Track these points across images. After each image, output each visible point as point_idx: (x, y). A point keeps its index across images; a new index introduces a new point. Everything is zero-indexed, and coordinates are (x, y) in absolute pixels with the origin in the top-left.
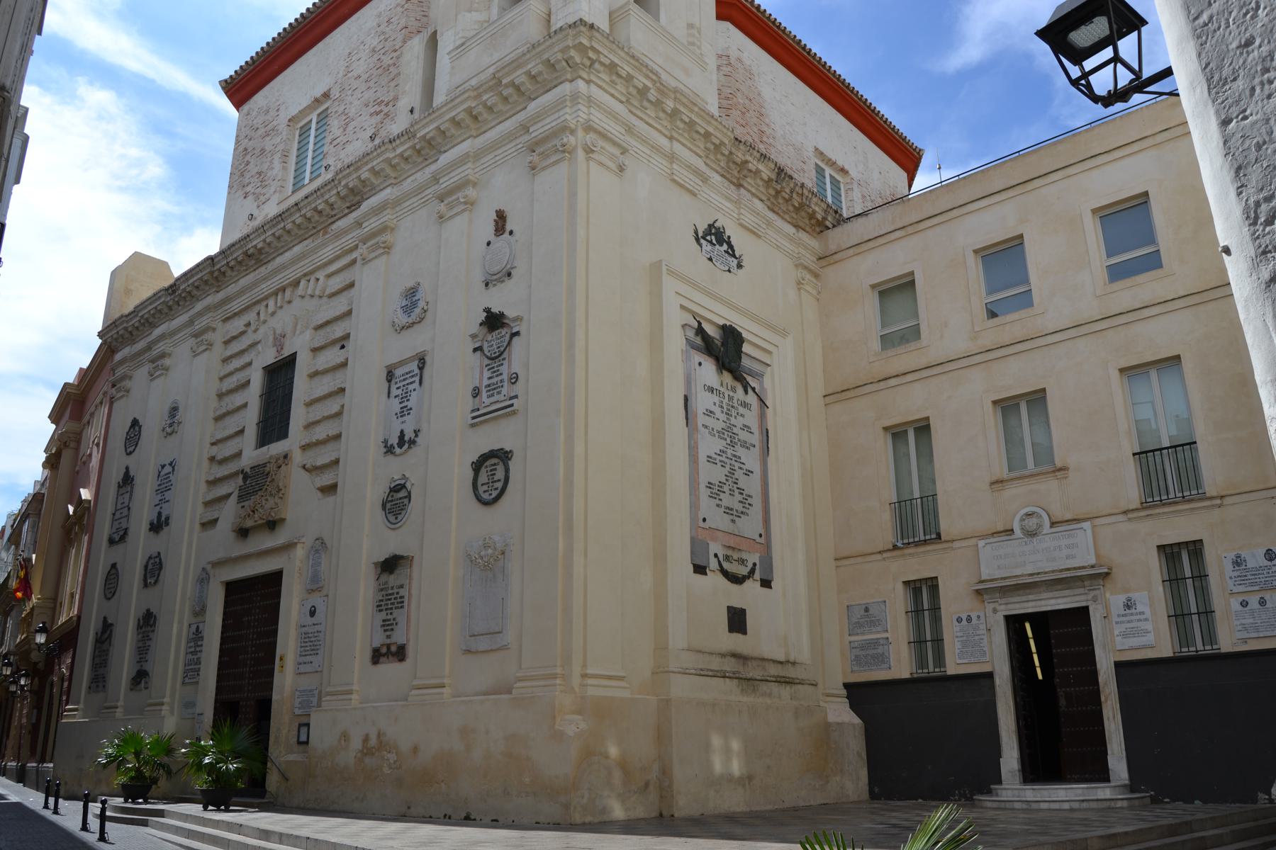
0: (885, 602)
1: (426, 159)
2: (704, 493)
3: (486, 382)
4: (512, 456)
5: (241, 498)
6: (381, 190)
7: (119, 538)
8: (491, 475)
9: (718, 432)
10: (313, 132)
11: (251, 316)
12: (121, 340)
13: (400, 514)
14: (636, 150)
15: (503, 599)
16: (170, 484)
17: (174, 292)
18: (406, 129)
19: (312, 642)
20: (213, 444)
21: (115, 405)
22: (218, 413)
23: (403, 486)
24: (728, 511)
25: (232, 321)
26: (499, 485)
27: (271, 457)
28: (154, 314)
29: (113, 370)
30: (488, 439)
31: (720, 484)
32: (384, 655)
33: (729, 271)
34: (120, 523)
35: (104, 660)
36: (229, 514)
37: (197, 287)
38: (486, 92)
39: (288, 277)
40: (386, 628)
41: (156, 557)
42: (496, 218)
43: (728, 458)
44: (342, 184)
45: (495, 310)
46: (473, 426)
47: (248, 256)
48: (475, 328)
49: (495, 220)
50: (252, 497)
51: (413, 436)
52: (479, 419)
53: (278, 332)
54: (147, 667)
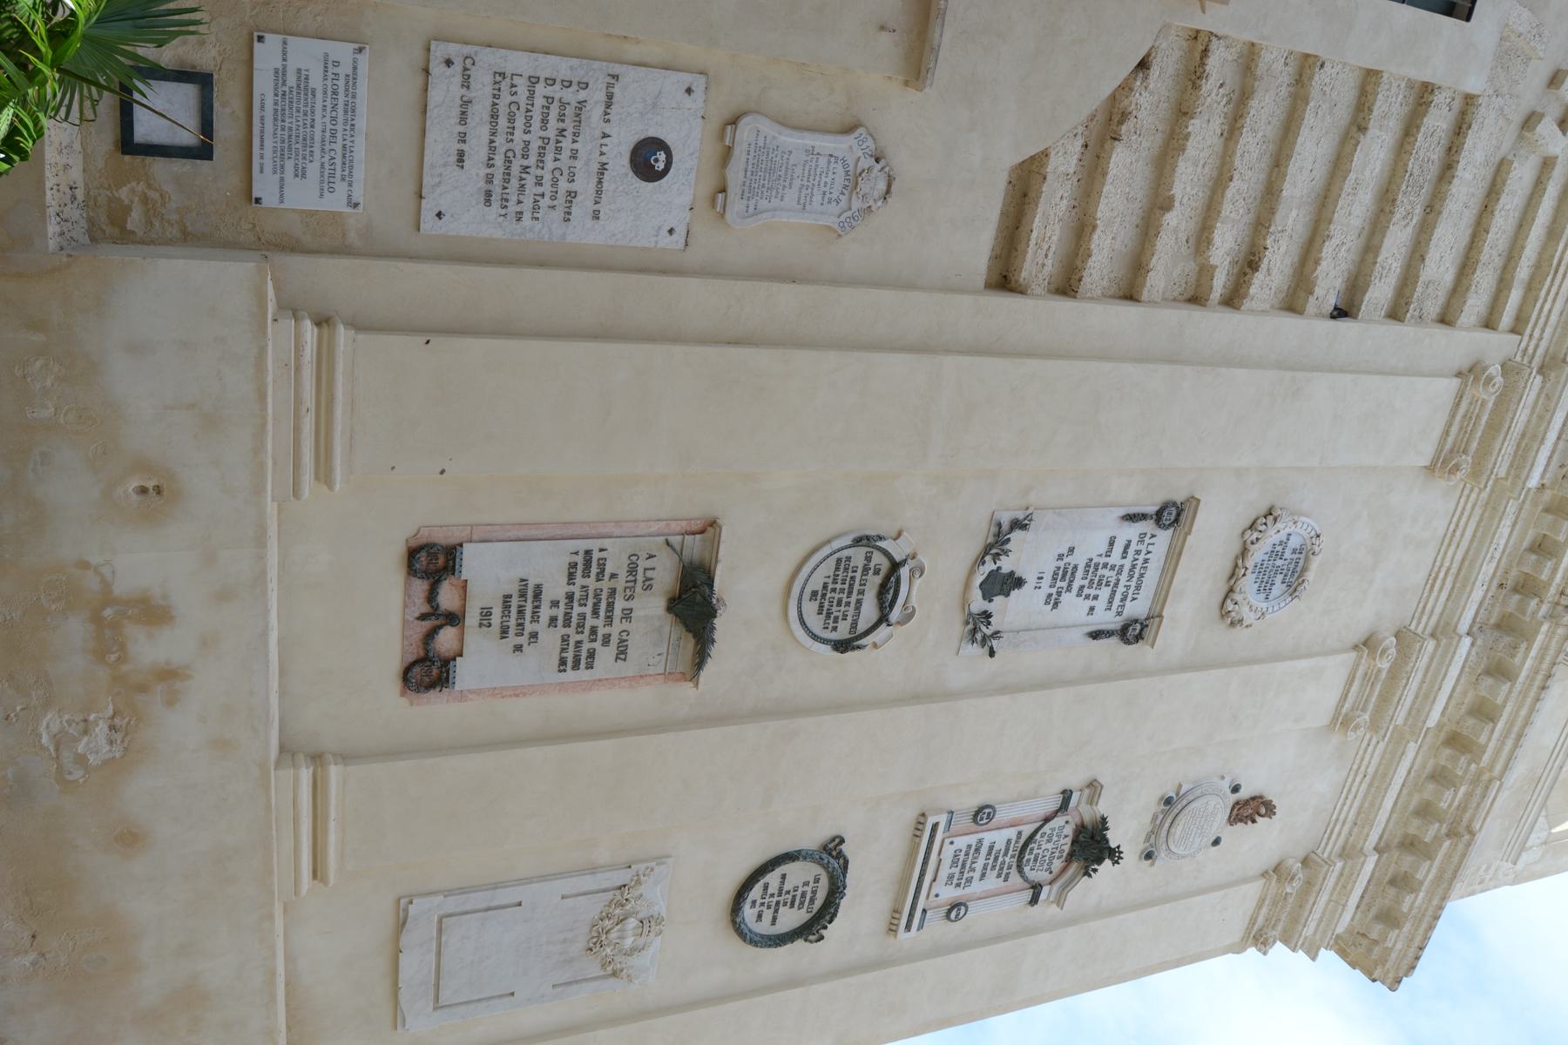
15: (512, 994)
19: (541, 162)
32: (432, 596)
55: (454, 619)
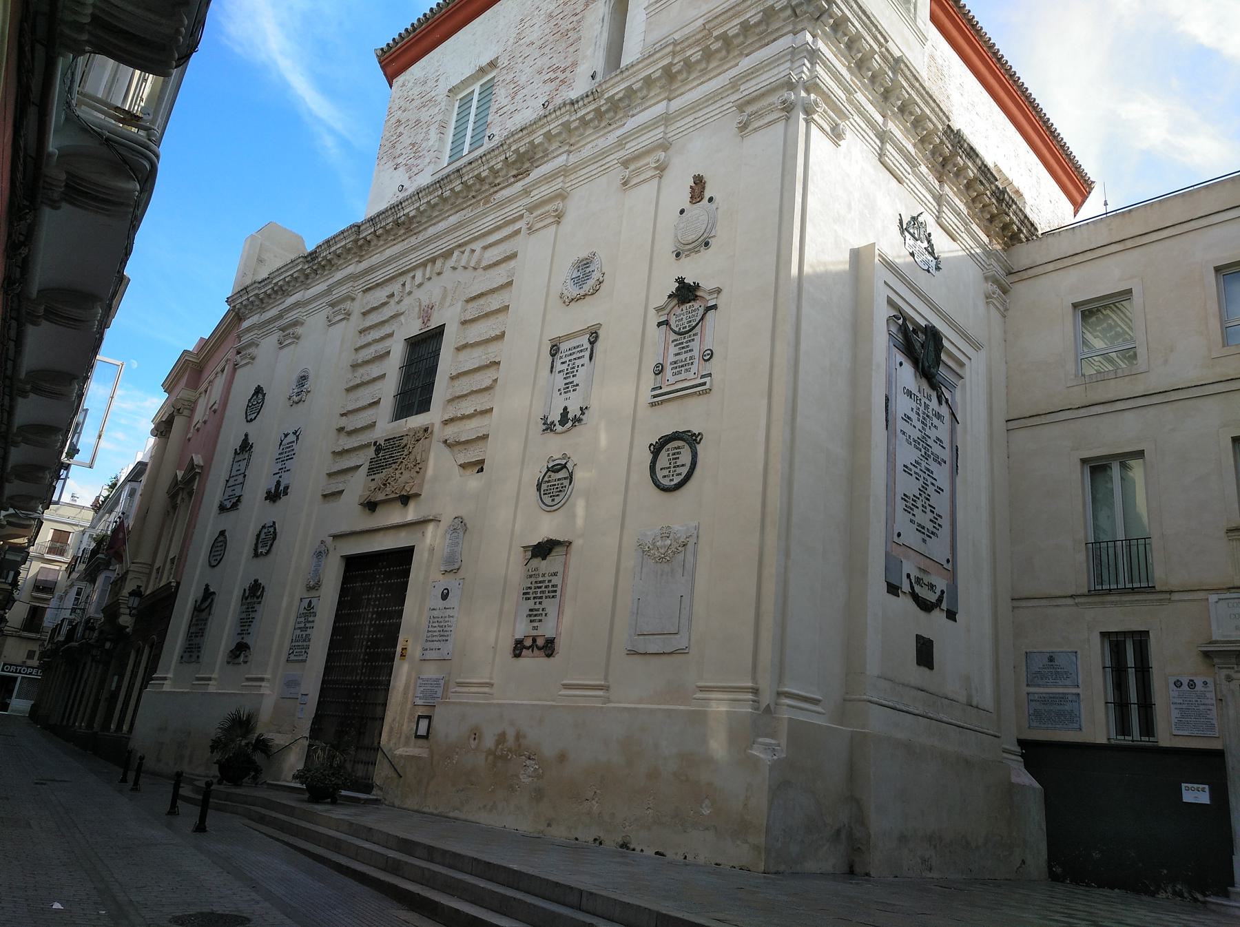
0: (1076, 652)
1: (610, 125)
2: (900, 505)
3: (671, 358)
4: (701, 440)
5: (372, 471)
6: (555, 157)
7: (230, 505)
8: (676, 459)
9: (915, 441)
10: (475, 103)
11: (395, 287)
12: (250, 307)
13: (558, 495)
14: (852, 121)
16: (292, 453)
17: (313, 259)
18: (593, 89)
19: (442, 627)
20: (342, 415)
21: (239, 372)
22: (351, 384)
23: (564, 466)
24: (921, 528)
25: (372, 292)
26: (684, 471)
27: (410, 430)
28: (288, 282)
29: (239, 337)
30: (671, 420)
31: (914, 498)
32: (528, 648)
33: (929, 271)
34: (234, 490)
35: (200, 629)
36: (357, 486)
37: (339, 256)
38: (690, 46)
39: (440, 247)
40: (532, 618)
41: (271, 527)
42: (693, 185)
43: (921, 470)
44: (513, 149)
45: (689, 280)
46: (653, 405)
47: (397, 224)
48: (661, 299)
49: (691, 187)
50: (384, 471)
51: (578, 413)
52: (660, 399)
53: (424, 304)
54: (247, 640)
55: (534, 640)
